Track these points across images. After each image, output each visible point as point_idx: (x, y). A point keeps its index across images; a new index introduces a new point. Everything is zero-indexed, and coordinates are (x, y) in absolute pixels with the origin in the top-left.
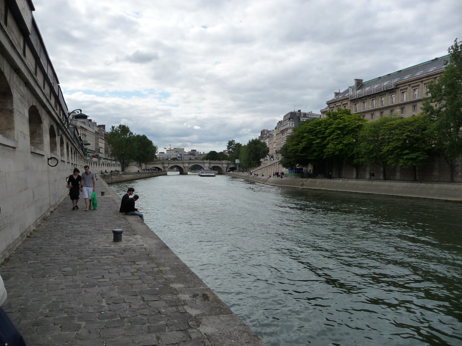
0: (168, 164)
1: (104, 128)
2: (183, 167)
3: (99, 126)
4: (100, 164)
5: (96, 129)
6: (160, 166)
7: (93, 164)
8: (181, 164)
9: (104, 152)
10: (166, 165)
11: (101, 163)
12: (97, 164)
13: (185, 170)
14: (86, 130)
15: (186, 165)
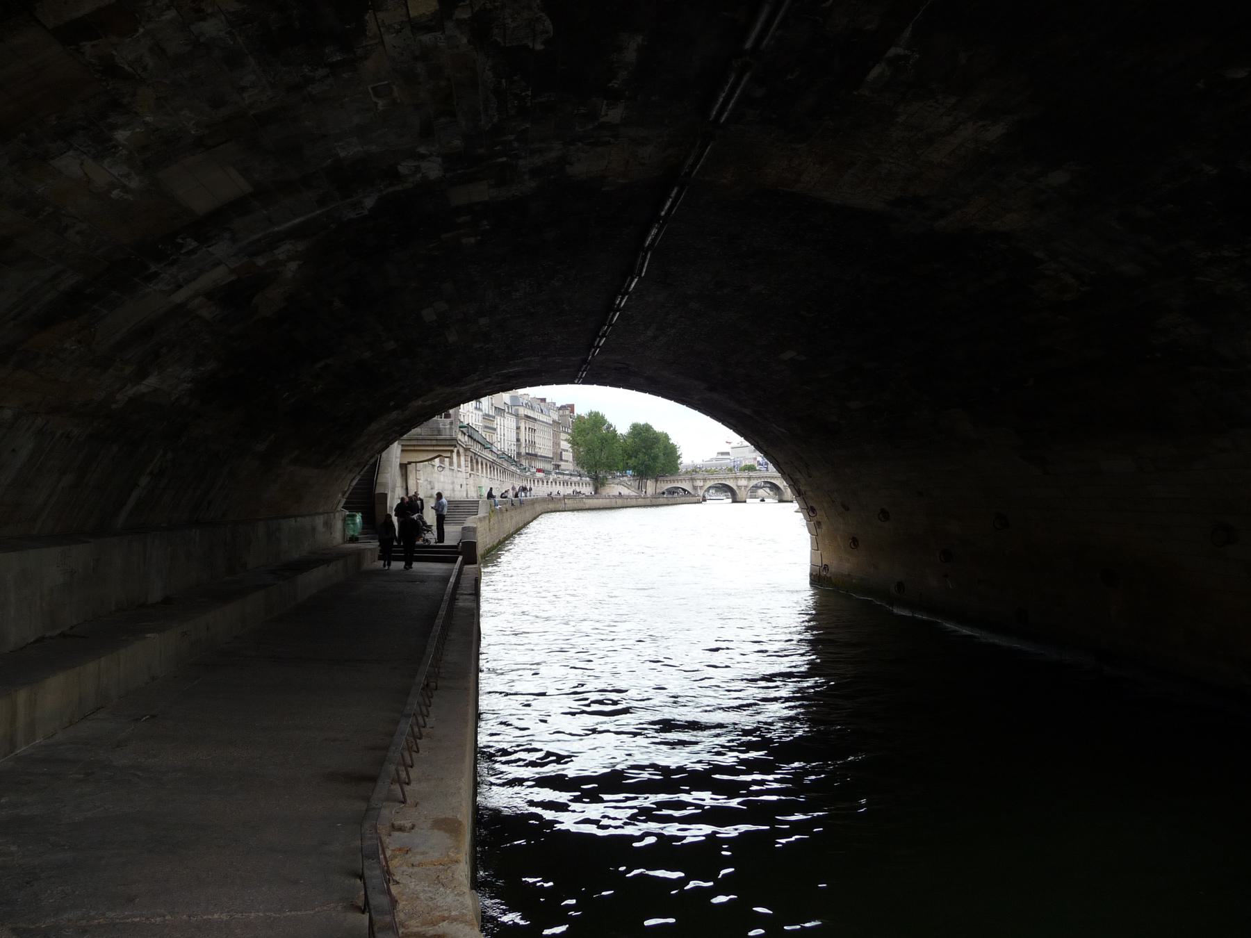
0: (702, 481)
1: (572, 411)
2: (735, 488)
3: (563, 408)
4: (550, 482)
5: (555, 416)
6: (687, 486)
7: (536, 482)
8: (732, 480)
9: (571, 459)
10: (699, 483)
11: (551, 480)
12: (543, 482)
13: (741, 494)
14: (535, 419)
15: (743, 482)
